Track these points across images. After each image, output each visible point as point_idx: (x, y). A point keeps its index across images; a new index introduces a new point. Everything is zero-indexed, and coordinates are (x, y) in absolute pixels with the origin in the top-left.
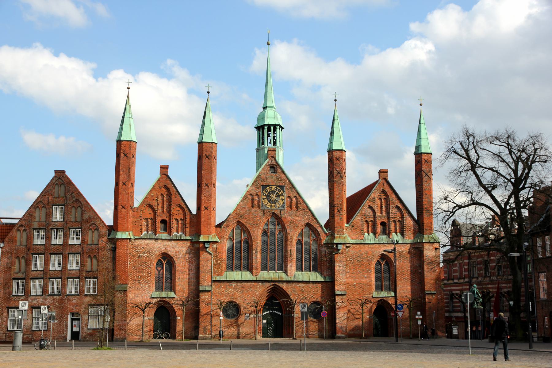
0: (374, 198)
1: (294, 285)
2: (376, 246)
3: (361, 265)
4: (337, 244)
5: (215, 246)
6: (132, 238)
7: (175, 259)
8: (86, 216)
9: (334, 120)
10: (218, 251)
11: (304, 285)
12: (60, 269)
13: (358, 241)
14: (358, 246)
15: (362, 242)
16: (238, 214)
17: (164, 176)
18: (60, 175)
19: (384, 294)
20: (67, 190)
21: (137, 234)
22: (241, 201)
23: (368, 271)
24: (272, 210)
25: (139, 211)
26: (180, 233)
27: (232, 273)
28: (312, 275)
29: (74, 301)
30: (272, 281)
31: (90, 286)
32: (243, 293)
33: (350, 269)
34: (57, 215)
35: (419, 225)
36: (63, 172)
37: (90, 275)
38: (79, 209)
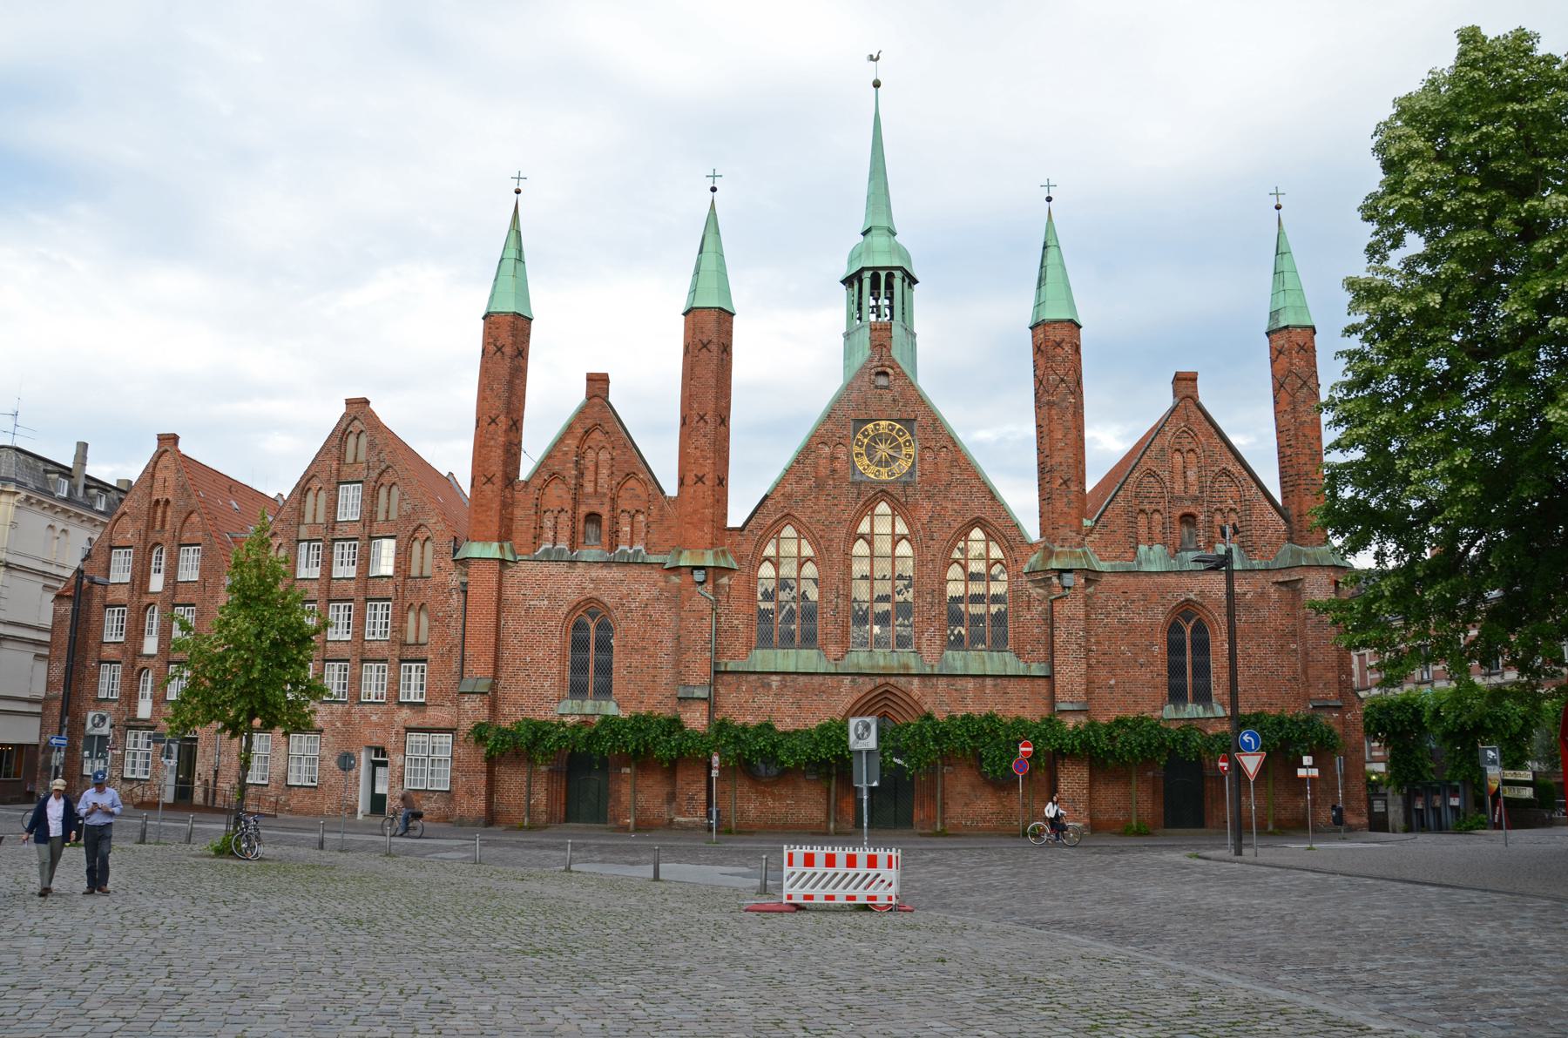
0: (1162, 449)
1: (942, 683)
2: (1172, 580)
3: (1129, 631)
4: (1061, 572)
5: (725, 580)
6: (509, 557)
7: (617, 614)
8: (407, 507)
9: (1045, 247)
10: (733, 593)
11: (971, 684)
12: (348, 637)
13: (1119, 565)
14: (1120, 580)
15: (1134, 566)
16: (788, 497)
17: (596, 400)
18: (358, 409)
19: (1193, 710)
20: (372, 445)
21: (524, 550)
22: (797, 461)
23: (1148, 648)
24: (881, 483)
25: (531, 489)
26: (639, 547)
27: (769, 653)
28: (991, 658)
29: (374, 718)
30: (879, 675)
31: (413, 684)
32: (799, 707)
33: (1098, 643)
34: (350, 504)
35: (1287, 520)
36: (367, 402)
37: (409, 654)
38: (394, 489)
